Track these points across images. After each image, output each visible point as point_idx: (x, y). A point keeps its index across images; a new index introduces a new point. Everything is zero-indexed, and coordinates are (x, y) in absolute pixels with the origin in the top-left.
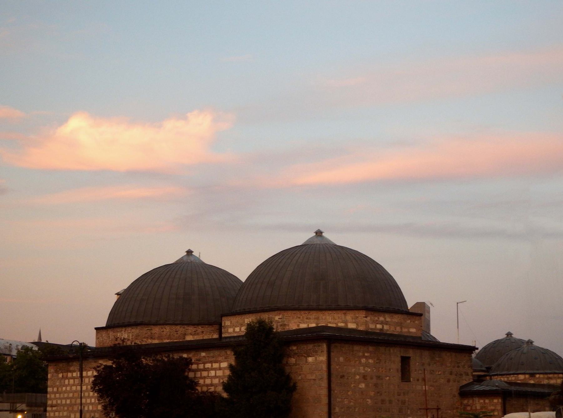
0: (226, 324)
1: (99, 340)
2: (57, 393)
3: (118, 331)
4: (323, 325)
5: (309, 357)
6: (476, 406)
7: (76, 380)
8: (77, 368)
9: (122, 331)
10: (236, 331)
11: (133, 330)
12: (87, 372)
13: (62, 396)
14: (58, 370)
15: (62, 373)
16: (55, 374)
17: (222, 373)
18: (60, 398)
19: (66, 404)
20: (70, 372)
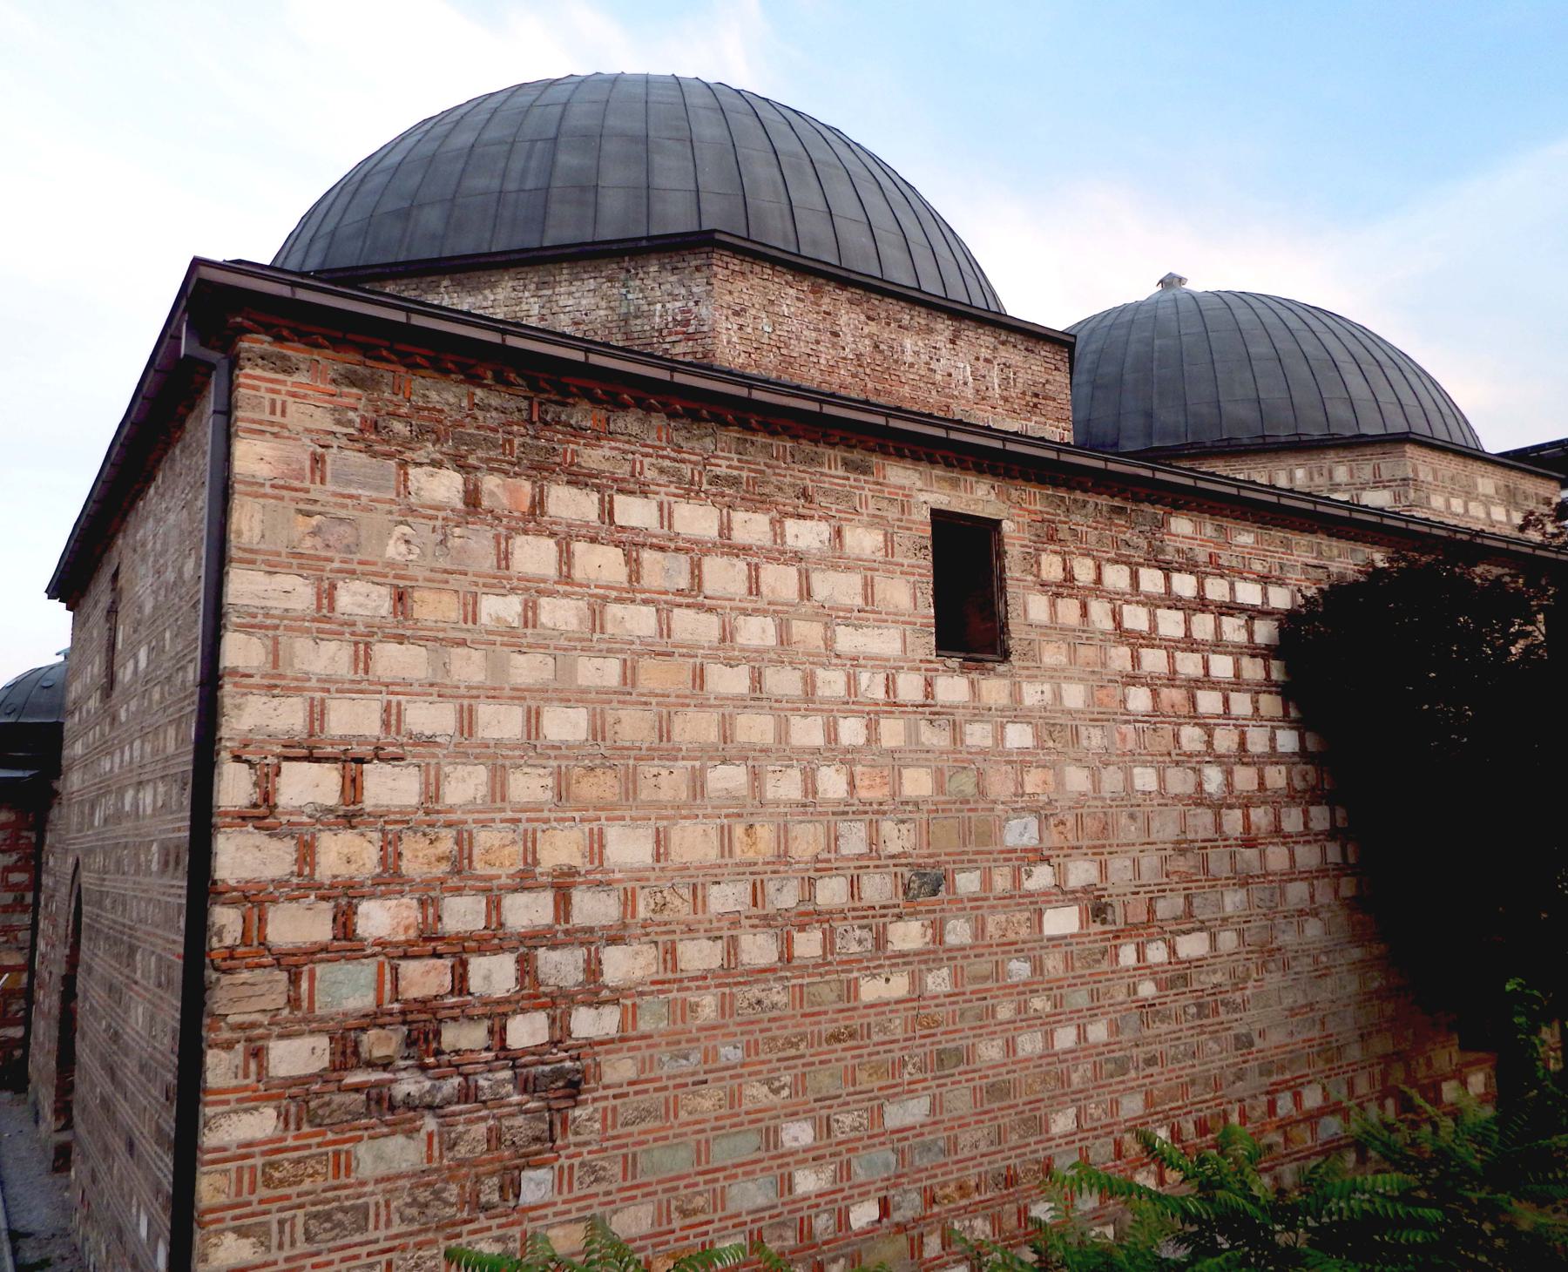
1: (741, 321)
2: (401, 639)
3: (904, 323)
7: (647, 556)
8: (662, 471)
9: (930, 331)
15: (462, 467)
18: (437, 690)
20: (578, 479)
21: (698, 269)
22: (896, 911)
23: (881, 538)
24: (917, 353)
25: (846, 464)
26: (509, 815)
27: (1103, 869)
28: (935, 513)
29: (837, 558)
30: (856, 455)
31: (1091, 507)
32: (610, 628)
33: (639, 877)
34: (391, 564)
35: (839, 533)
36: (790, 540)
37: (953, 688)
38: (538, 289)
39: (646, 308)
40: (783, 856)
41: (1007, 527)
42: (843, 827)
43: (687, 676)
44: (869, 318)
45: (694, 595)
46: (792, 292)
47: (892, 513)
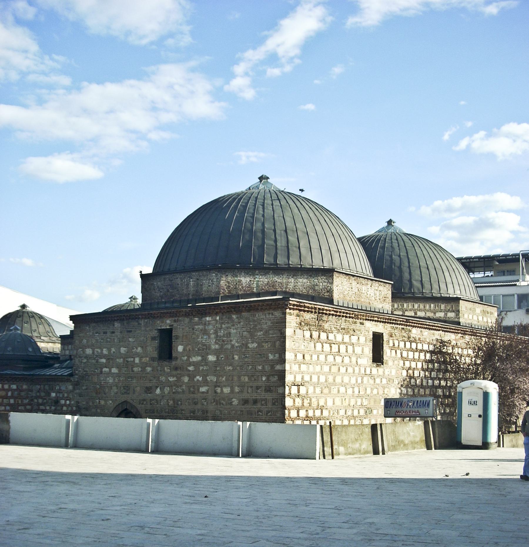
2: (304, 364)
3: (363, 283)
7: (333, 345)
9: (367, 284)
21: (330, 276)
22: (364, 417)
24: (365, 290)
26: (316, 396)
28: (373, 332)
31: (398, 328)
37: (374, 370)
38: (293, 276)
39: (318, 284)
40: (349, 405)
41: (384, 334)
42: (358, 399)
43: (337, 369)
44: (358, 283)
47: (367, 333)
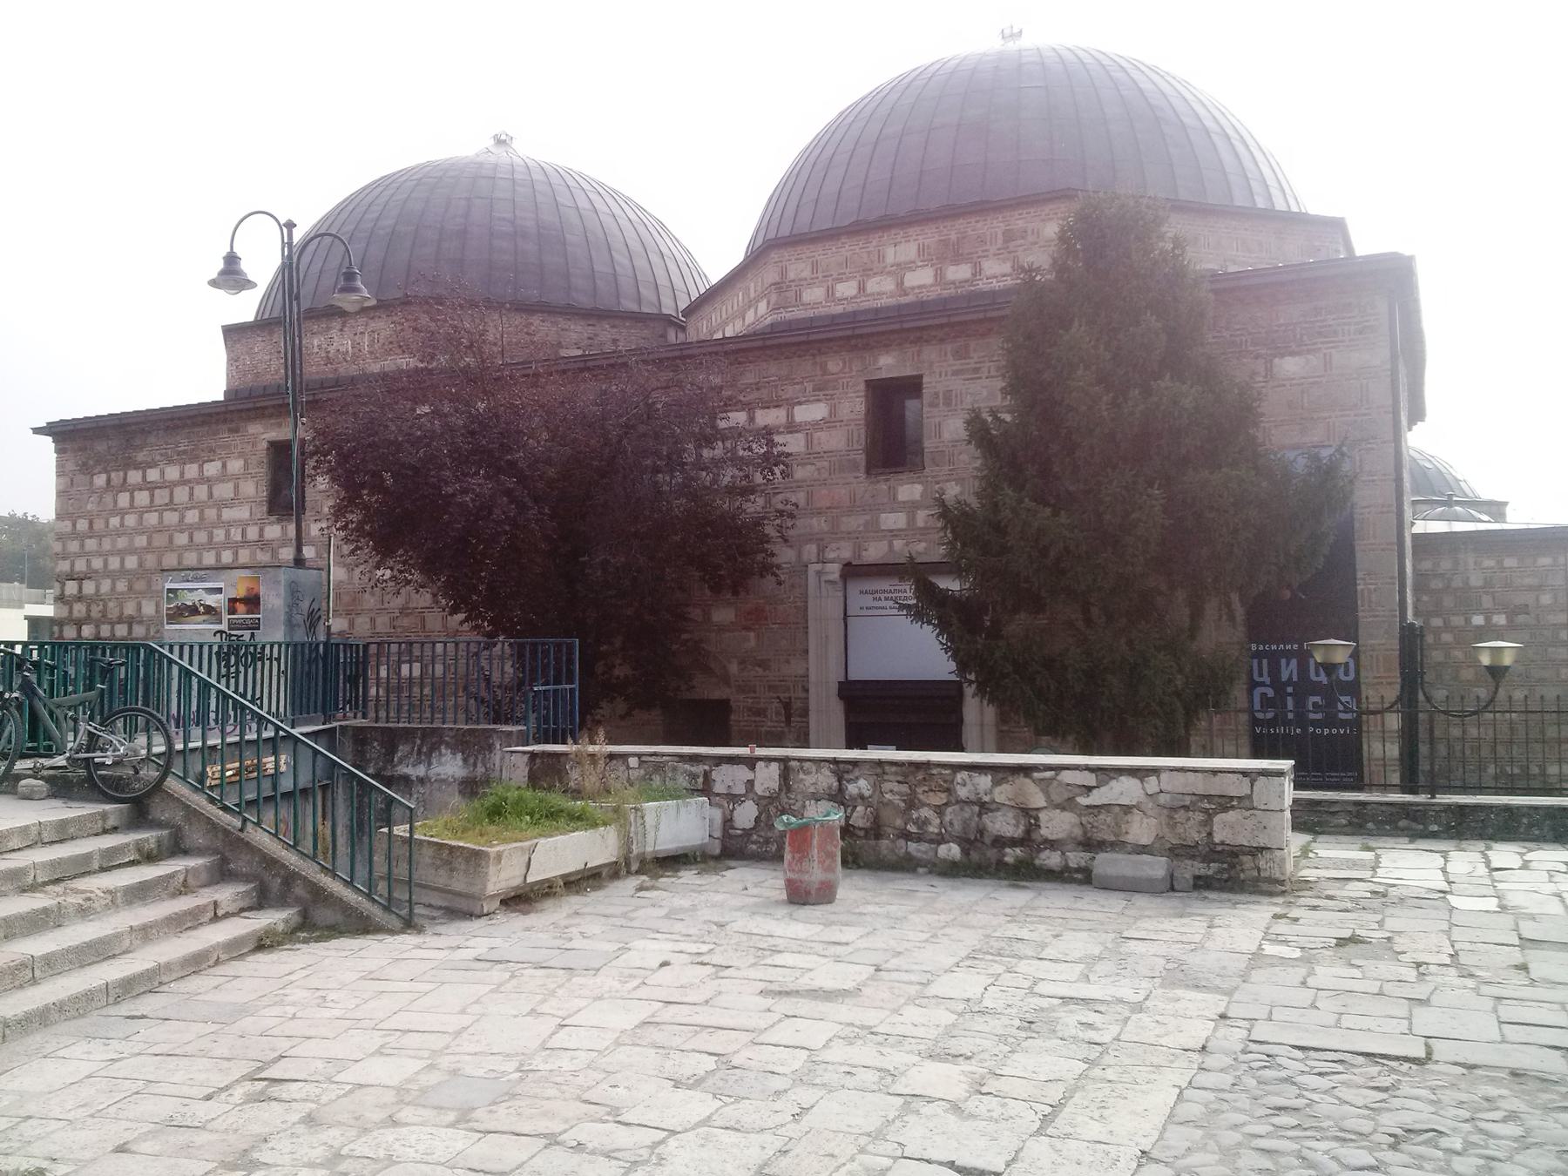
0: (791, 275)
2: (91, 537)
4: (1210, 266)
5: (1283, 356)
6: (1468, 578)
8: (162, 455)
9: (329, 329)
10: (838, 295)
11: (373, 325)
12: (201, 467)
13: (107, 544)
14: (91, 462)
16: (80, 478)
17: (803, 443)
18: (99, 554)
19: (123, 571)
23: (243, 462)
25: (231, 431)
27: (352, 624)
29: (224, 477)
30: (233, 425)
32: (145, 524)
33: (151, 619)
34: (89, 512)
35: (224, 466)
36: (205, 473)
45: (171, 505)
46: (260, 339)
